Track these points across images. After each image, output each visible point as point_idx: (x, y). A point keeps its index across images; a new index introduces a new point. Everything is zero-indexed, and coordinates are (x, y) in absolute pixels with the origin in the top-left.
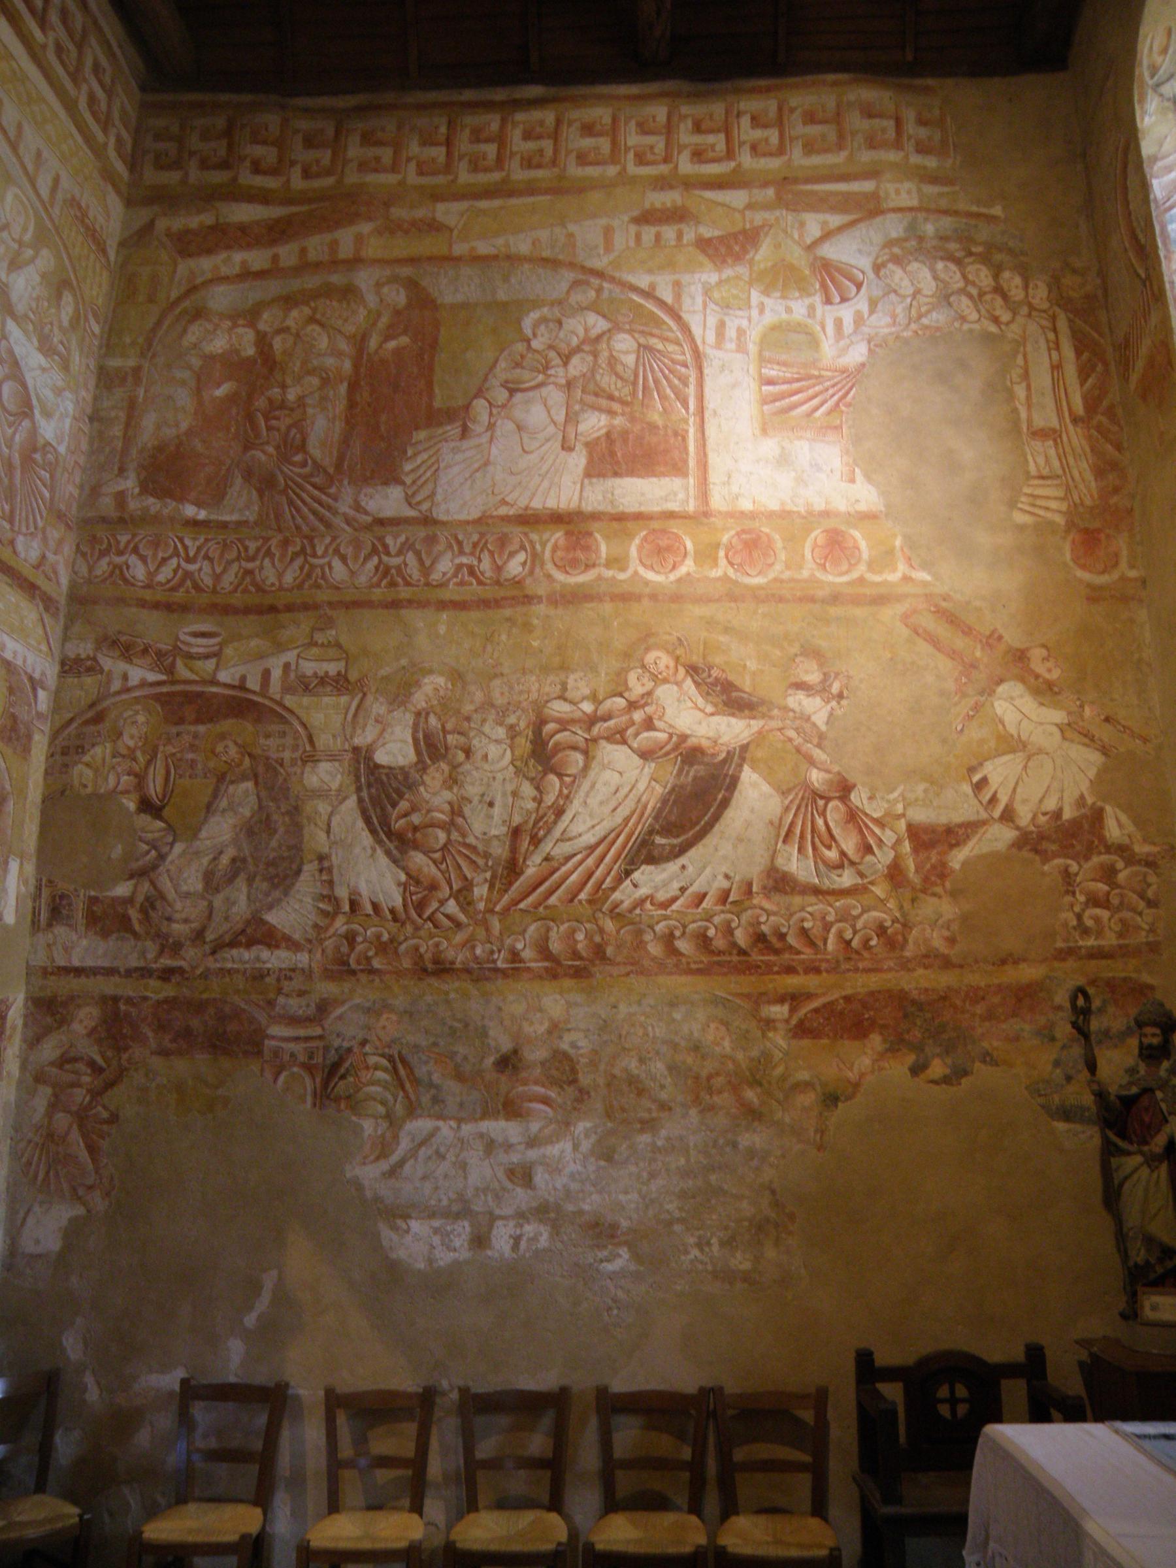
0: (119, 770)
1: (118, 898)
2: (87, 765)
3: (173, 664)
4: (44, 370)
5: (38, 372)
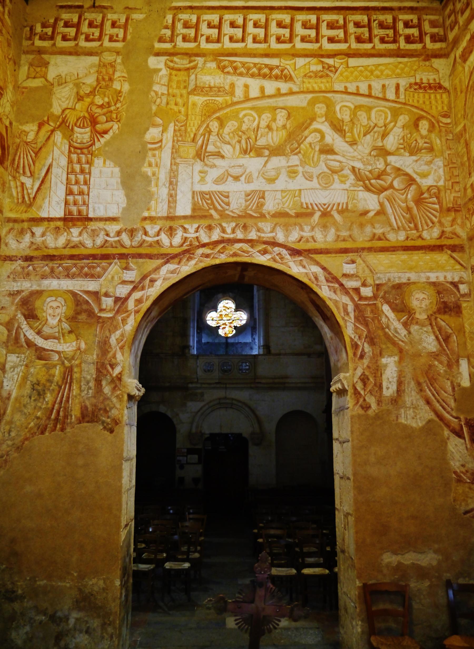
4: (416, 161)
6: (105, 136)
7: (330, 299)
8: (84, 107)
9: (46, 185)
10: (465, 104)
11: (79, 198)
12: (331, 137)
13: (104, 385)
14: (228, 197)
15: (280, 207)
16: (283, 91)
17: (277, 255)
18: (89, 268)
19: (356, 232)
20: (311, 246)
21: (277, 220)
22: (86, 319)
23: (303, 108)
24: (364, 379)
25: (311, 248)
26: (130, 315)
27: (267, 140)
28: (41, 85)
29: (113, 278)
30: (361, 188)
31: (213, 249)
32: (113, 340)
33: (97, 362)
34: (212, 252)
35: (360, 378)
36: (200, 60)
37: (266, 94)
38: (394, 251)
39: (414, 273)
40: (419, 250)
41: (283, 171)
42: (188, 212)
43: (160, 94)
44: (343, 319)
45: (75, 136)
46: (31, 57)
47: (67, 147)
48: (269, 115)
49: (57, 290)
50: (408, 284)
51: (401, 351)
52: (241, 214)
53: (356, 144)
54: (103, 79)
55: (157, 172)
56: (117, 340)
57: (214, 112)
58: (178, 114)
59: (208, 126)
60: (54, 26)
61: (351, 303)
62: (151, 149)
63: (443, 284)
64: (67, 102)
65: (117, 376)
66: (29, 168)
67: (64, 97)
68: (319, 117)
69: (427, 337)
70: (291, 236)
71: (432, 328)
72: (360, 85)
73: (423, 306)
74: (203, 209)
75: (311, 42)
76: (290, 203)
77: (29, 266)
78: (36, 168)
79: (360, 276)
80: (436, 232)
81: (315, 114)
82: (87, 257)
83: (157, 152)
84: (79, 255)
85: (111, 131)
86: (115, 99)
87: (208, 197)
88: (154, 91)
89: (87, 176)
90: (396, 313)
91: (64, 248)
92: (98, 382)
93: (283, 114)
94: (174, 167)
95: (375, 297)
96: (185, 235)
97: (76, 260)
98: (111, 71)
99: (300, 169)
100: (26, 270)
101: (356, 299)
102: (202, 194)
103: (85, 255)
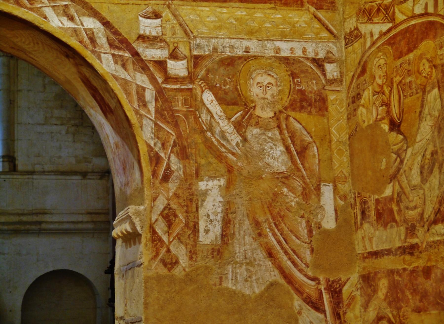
0: (377, 104)
1: (387, 197)
2: (363, 106)
3: (394, 13)
7: (116, 78)
24: (168, 216)
35: (161, 214)
39: (256, 41)
44: (137, 112)
51: (230, 170)
61: (151, 87)
63: (300, 62)
69: (271, 148)
71: (281, 133)
73: (268, 96)
79: (168, 40)
90: (225, 106)
95: (191, 78)
101: (160, 80)
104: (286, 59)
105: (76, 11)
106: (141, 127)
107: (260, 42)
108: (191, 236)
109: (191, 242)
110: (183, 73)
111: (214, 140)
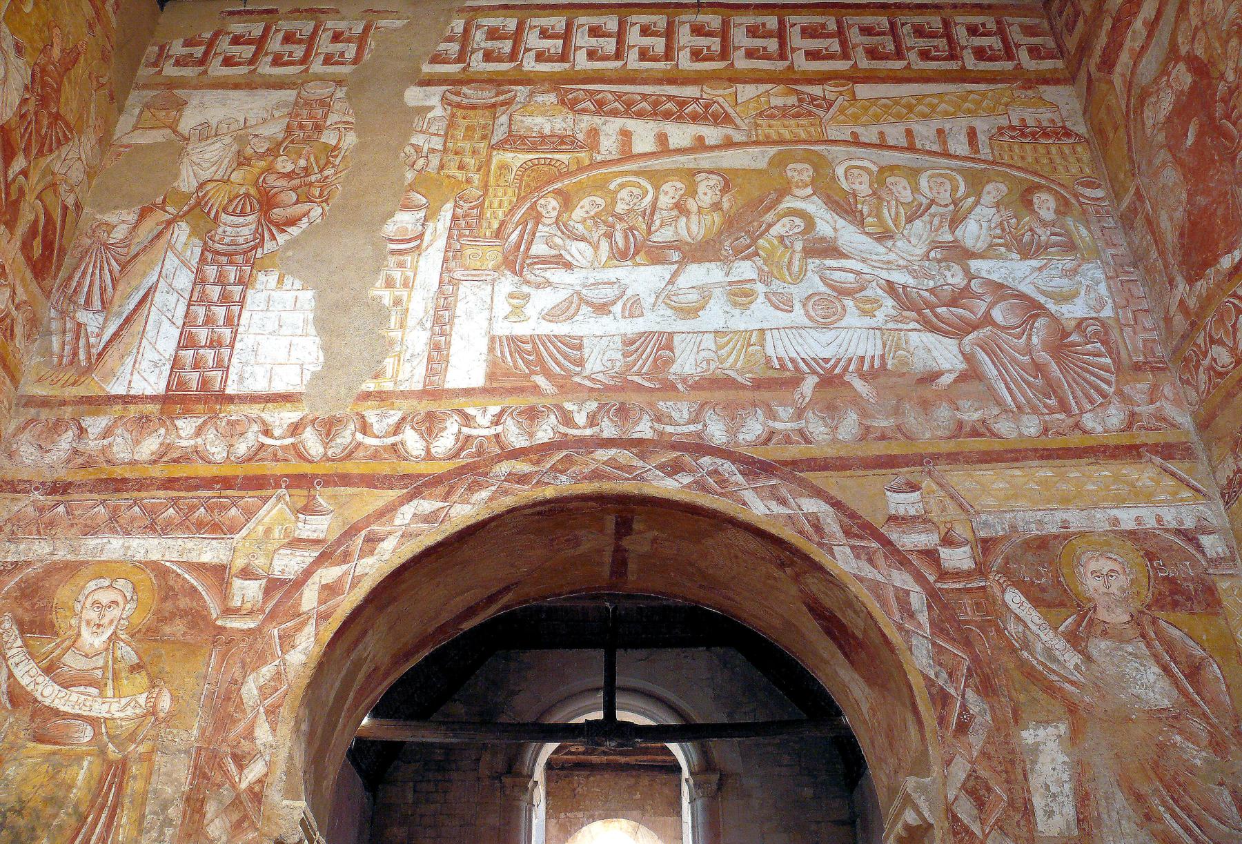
4: (1040, 269)
5: (1036, 274)
6: (289, 229)
8: (248, 177)
9: (137, 327)
10: (1130, 149)
11: (209, 354)
12: (827, 223)
13: (209, 816)
14: (580, 347)
15: (713, 366)
16: (710, 141)
17: (709, 474)
18: (209, 509)
19: (912, 419)
20: (795, 451)
21: (704, 395)
22: (184, 634)
23: (760, 172)
24: (977, 791)
25: (798, 457)
26: (304, 623)
27: (677, 233)
28: (160, 140)
29: (268, 531)
30: (913, 325)
31: (538, 462)
32: (250, 690)
33: (199, 749)
34: (535, 469)
35: (964, 787)
36: (522, 91)
37: (671, 147)
38: (1017, 460)
40: (1080, 457)
41: (717, 292)
42: (477, 379)
43: (425, 149)
44: (900, 628)
45: (220, 231)
46: (149, 94)
47: (198, 251)
48: (679, 185)
49: (116, 562)
50: (1066, 537)
51: (1072, 709)
52: (612, 383)
53: (891, 237)
54: (301, 127)
55: (405, 299)
56: (261, 688)
57: (549, 182)
58: (465, 185)
59: (533, 207)
60: (211, 44)
61: (918, 589)
62: (392, 253)
63: (1155, 536)
64: (214, 169)
65: (250, 788)
66: (102, 294)
67: (206, 161)
68: (797, 187)
69: (1138, 670)
70: (744, 429)
71: (1149, 645)
72: (887, 129)
74: (514, 375)
75: (769, 58)
76: (736, 361)
77: (56, 506)
78: (118, 293)
79: (935, 519)
80: (1115, 417)
81: (789, 182)
82: (208, 483)
83: (408, 258)
84: (187, 478)
85: (305, 220)
86: (322, 162)
87: (529, 347)
88: (413, 145)
89: (236, 309)
90: (1044, 610)
91: (155, 462)
92: (194, 804)
93: (712, 183)
94: (448, 289)
95: (981, 570)
96: (466, 430)
97: (179, 490)
98: (320, 113)
99: (760, 288)
100: (48, 515)
101: (931, 579)
102: (512, 340)
103: (203, 479)
104: (1132, 534)
105: (789, 492)
106: (910, 649)
107: (1085, 513)
108: (1022, 823)
109: (1024, 832)
110: (968, 564)
111: (1035, 663)
